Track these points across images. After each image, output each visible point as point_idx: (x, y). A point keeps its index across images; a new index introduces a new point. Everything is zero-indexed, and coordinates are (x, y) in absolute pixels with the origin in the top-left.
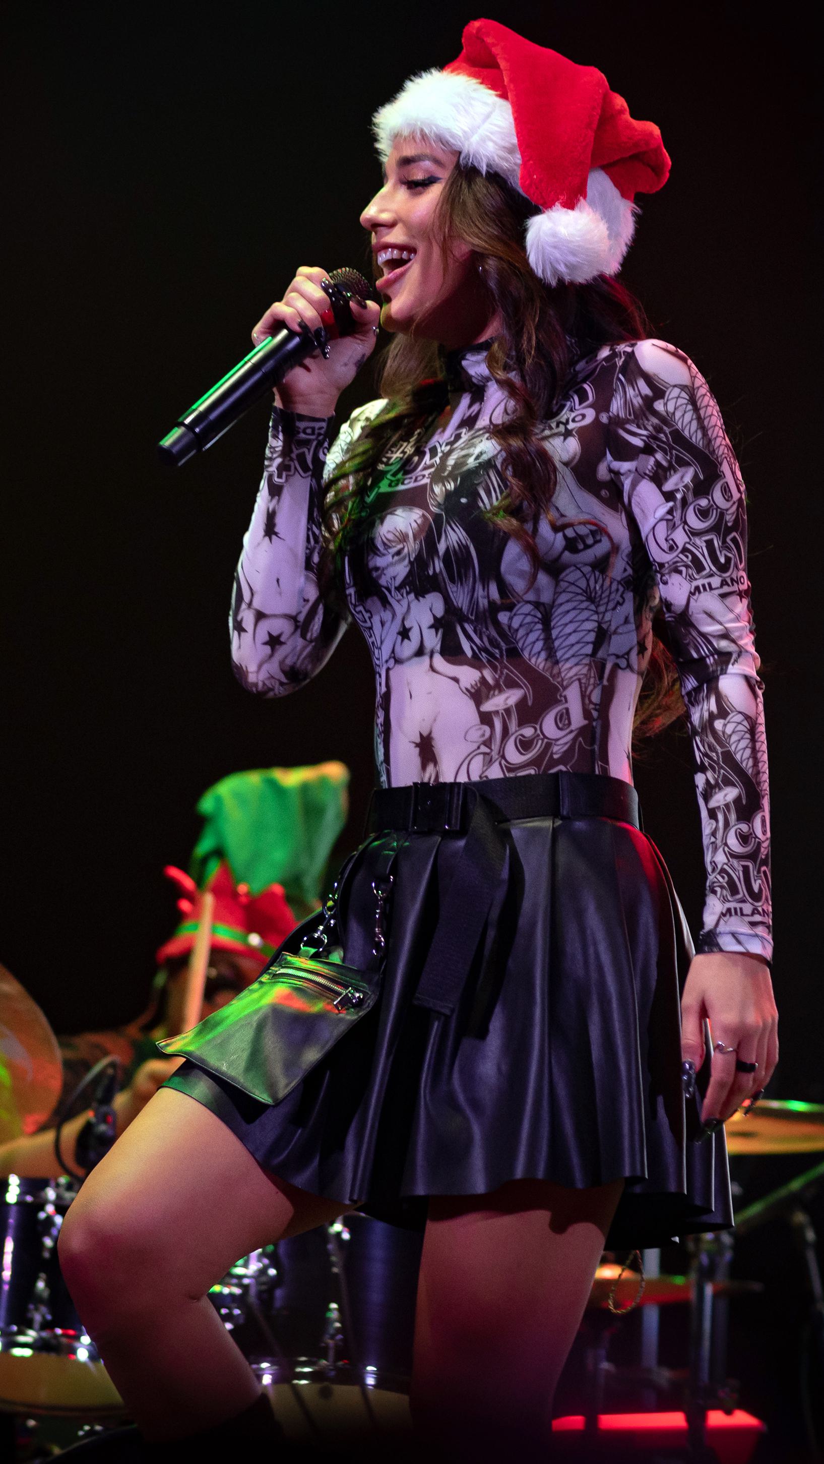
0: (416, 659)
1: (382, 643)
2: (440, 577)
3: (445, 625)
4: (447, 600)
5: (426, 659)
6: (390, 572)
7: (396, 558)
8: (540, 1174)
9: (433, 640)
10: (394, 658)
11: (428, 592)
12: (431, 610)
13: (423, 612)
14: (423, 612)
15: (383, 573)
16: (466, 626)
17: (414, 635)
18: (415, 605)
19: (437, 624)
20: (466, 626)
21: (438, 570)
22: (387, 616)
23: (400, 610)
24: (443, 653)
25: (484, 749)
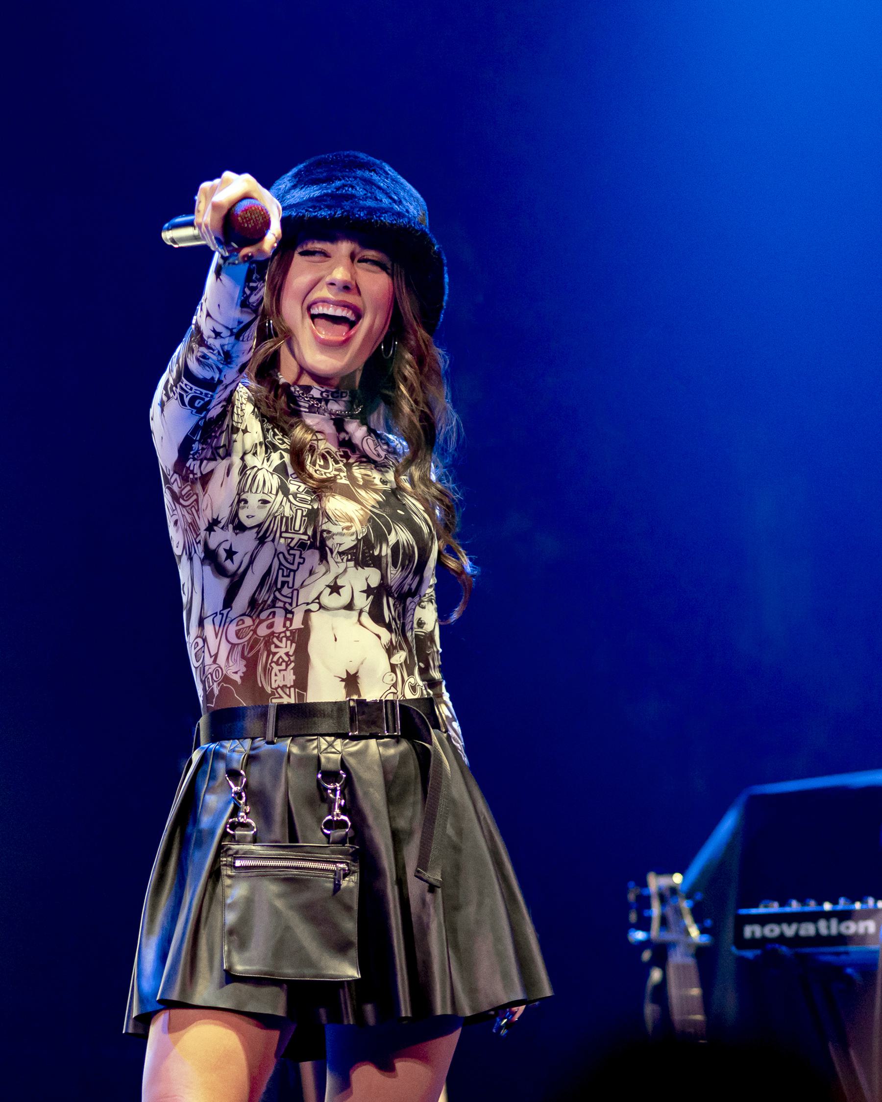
0: (343, 611)
1: (302, 586)
2: (384, 560)
3: (377, 594)
4: (384, 577)
5: (355, 614)
6: (337, 539)
7: (345, 531)
8: (547, 991)
9: (363, 602)
10: (319, 603)
11: (368, 566)
12: (366, 579)
13: (359, 580)
14: (359, 580)
15: (332, 537)
16: (390, 599)
18: (352, 570)
19: (369, 591)
20: (390, 599)
21: (383, 554)
22: (321, 569)
24: (370, 613)
25: (393, 690)
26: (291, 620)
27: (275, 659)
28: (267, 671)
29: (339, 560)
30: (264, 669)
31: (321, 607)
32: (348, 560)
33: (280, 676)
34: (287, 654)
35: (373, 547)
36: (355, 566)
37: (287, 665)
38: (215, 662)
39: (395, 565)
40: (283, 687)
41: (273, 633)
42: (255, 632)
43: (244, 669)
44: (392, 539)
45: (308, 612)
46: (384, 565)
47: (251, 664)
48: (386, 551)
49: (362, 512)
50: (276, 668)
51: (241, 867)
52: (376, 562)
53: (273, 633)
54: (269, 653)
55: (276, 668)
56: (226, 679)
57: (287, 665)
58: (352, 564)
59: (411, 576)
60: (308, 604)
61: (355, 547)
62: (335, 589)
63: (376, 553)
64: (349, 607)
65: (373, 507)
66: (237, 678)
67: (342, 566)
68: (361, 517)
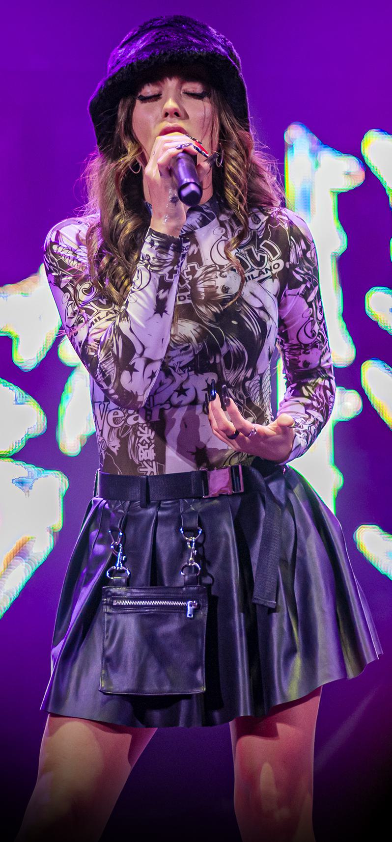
2: (219, 366)
21: (218, 361)
22: (169, 380)
26: (151, 416)
27: (141, 441)
28: (135, 449)
29: (182, 372)
30: (133, 446)
31: (172, 406)
32: (189, 371)
33: (145, 453)
34: (149, 438)
36: (196, 374)
37: (149, 446)
38: (102, 435)
40: (147, 461)
41: (138, 423)
42: (126, 421)
43: (119, 446)
44: (224, 350)
46: (219, 369)
47: (124, 442)
49: (198, 330)
50: (141, 448)
51: (117, 606)
52: (214, 368)
53: (138, 423)
54: (136, 436)
55: (141, 448)
56: (108, 450)
57: (149, 446)
60: (161, 405)
62: (182, 391)
63: (212, 362)
65: (210, 321)
66: (115, 450)
67: (185, 376)
68: (198, 335)
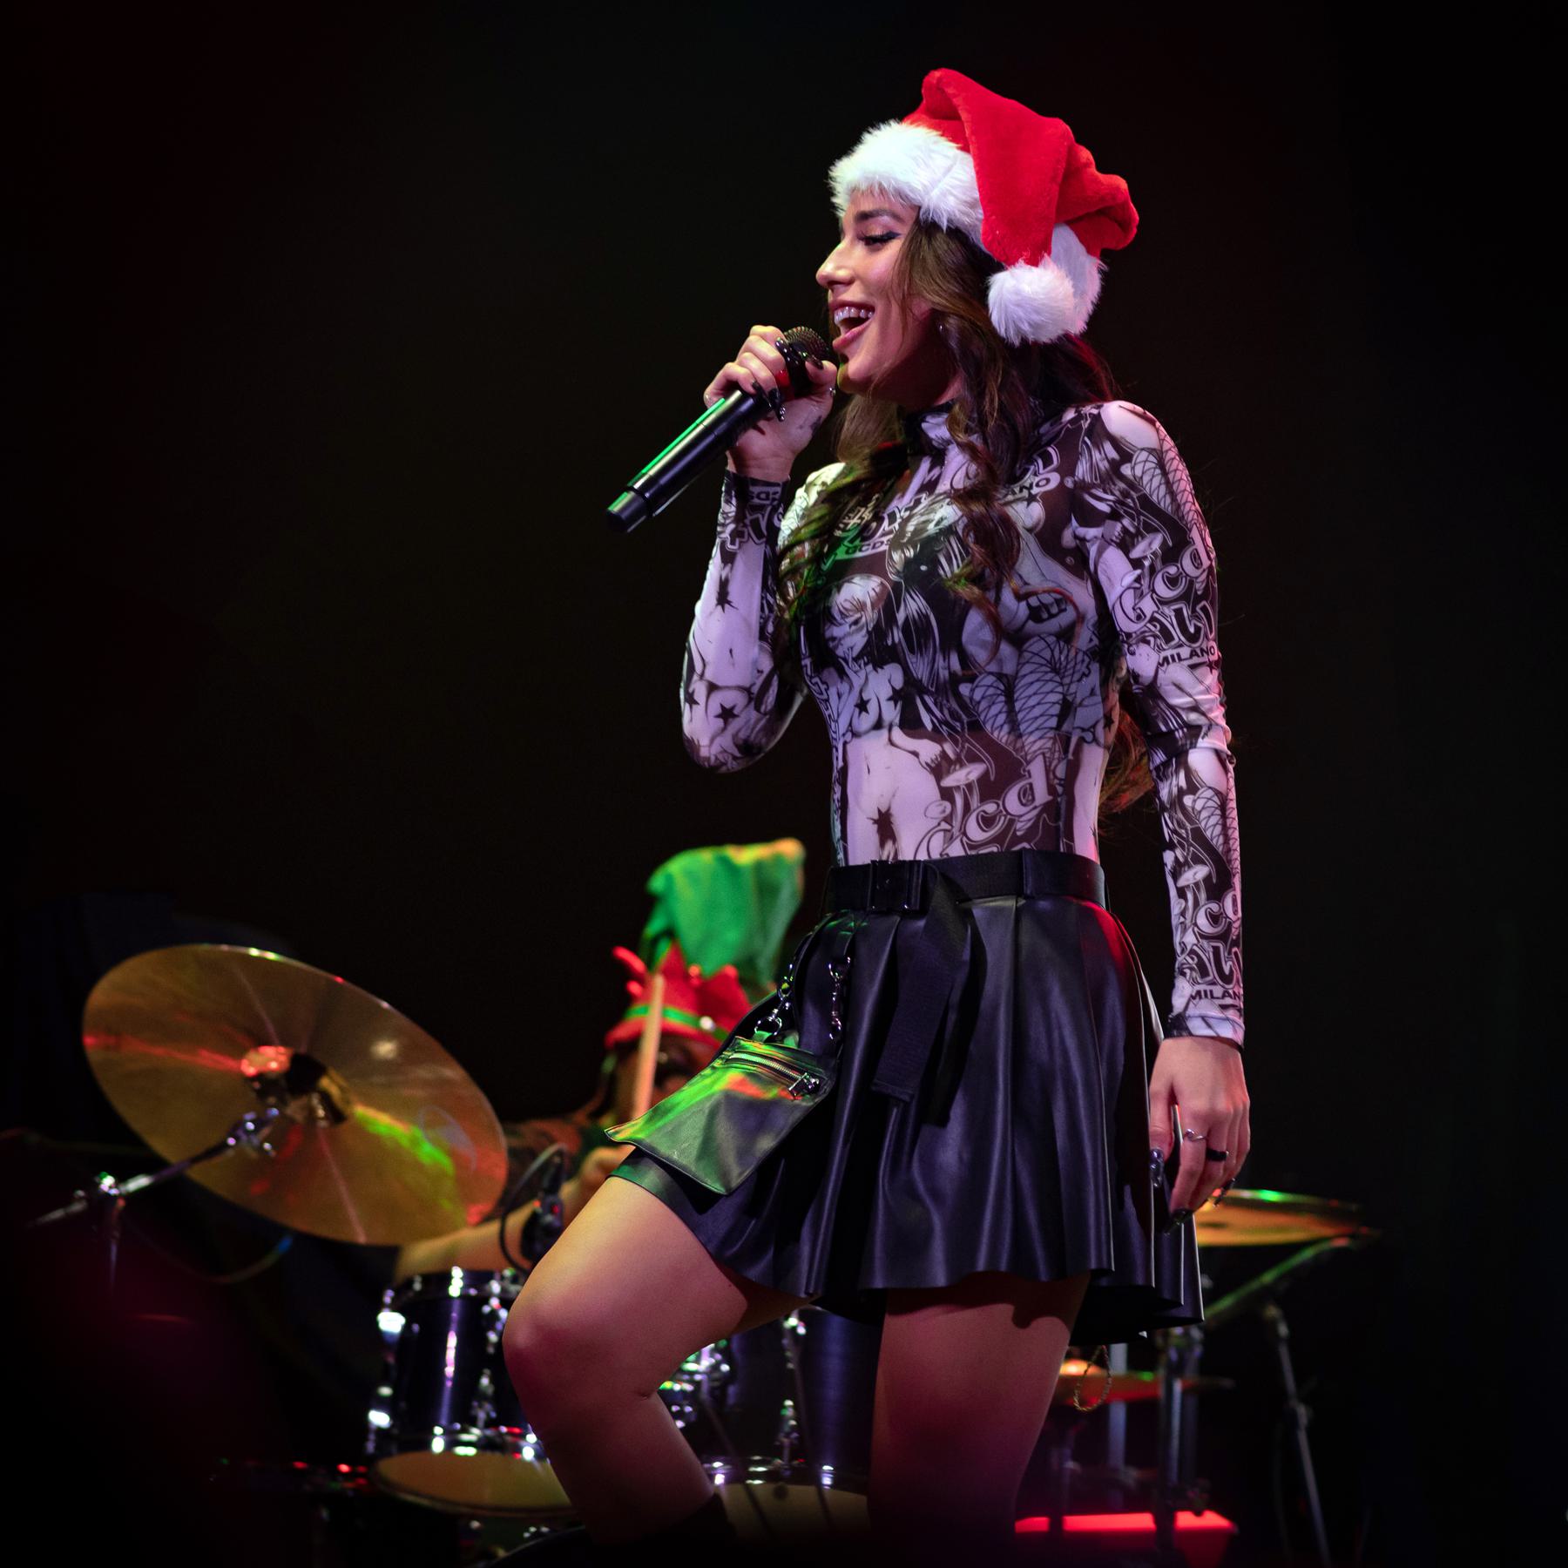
3: (905, 697)
4: (907, 671)
6: (848, 642)
9: (892, 713)
11: (887, 663)
13: (881, 684)
14: (881, 684)
16: (926, 698)
17: (872, 707)
18: (872, 675)
19: (896, 696)
20: (926, 698)
23: (857, 681)
24: (902, 726)
35: (885, 637)
39: (912, 651)
45: (845, 744)
48: (897, 635)
58: (870, 667)
59: (939, 658)
61: (868, 644)
64: (878, 725)
